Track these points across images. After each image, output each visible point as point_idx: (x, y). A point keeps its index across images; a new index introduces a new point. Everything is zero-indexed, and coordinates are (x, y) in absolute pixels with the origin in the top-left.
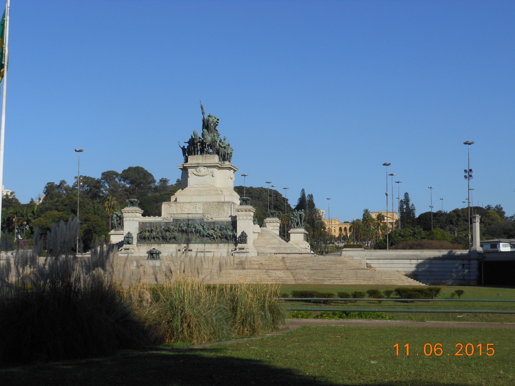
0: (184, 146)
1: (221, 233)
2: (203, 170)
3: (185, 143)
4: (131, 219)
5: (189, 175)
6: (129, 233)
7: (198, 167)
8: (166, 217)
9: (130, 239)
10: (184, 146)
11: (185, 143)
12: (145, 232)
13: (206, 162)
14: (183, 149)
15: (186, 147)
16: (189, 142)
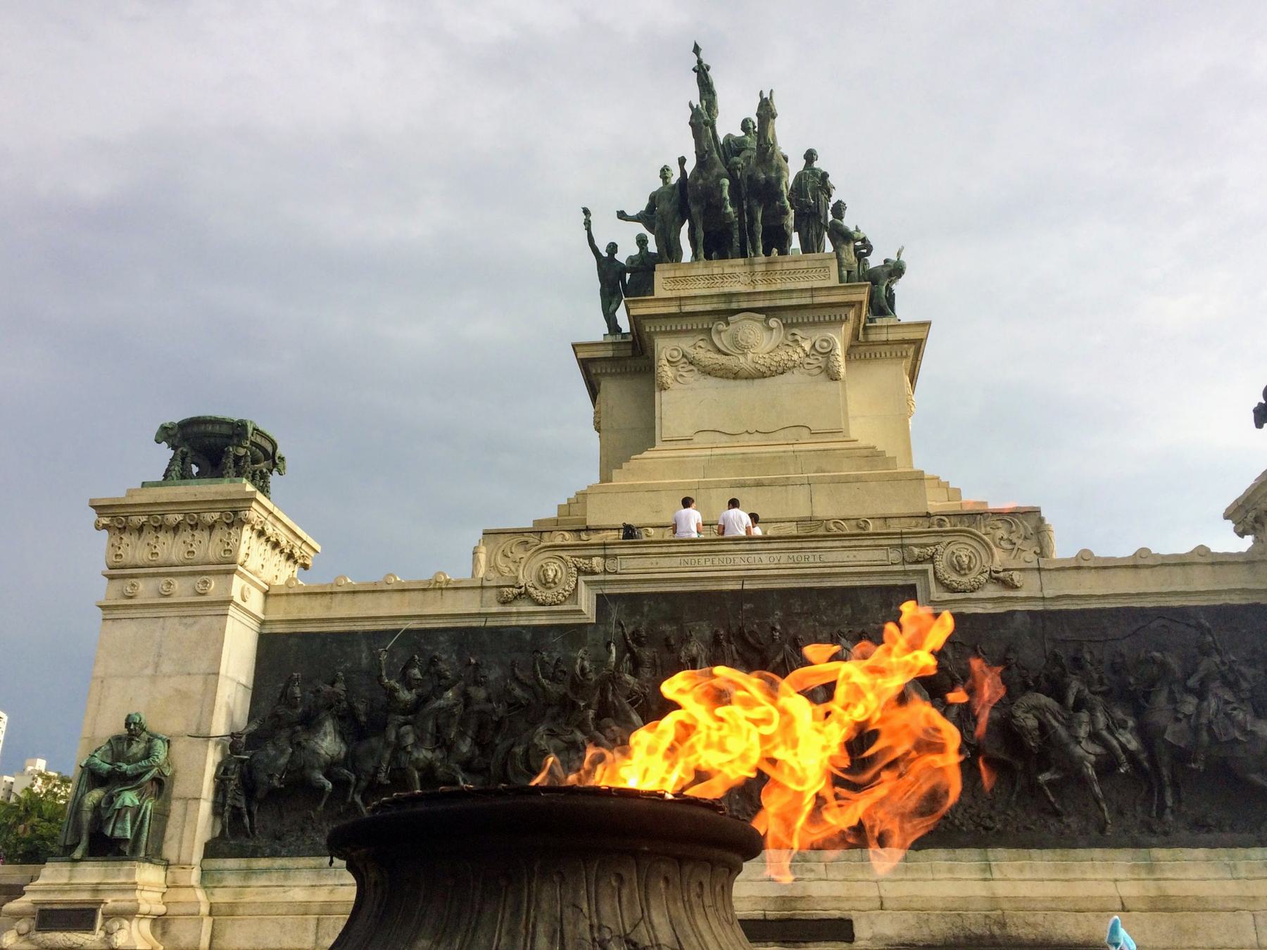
0: (613, 248)
1: (1143, 731)
2: (760, 341)
3: (622, 215)
4: (181, 589)
5: (666, 372)
6: (134, 729)
7: (724, 315)
8: (526, 577)
9: (129, 798)
10: (613, 248)
11: (622, 215)
12: (310, 722)
13: (779, 286)
14: (608, 268)
15: (621, 257)
16: (647, 217)
